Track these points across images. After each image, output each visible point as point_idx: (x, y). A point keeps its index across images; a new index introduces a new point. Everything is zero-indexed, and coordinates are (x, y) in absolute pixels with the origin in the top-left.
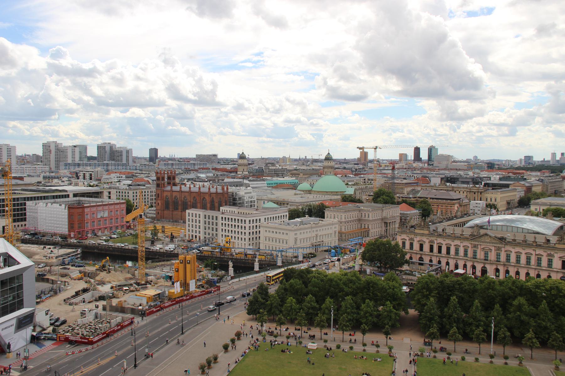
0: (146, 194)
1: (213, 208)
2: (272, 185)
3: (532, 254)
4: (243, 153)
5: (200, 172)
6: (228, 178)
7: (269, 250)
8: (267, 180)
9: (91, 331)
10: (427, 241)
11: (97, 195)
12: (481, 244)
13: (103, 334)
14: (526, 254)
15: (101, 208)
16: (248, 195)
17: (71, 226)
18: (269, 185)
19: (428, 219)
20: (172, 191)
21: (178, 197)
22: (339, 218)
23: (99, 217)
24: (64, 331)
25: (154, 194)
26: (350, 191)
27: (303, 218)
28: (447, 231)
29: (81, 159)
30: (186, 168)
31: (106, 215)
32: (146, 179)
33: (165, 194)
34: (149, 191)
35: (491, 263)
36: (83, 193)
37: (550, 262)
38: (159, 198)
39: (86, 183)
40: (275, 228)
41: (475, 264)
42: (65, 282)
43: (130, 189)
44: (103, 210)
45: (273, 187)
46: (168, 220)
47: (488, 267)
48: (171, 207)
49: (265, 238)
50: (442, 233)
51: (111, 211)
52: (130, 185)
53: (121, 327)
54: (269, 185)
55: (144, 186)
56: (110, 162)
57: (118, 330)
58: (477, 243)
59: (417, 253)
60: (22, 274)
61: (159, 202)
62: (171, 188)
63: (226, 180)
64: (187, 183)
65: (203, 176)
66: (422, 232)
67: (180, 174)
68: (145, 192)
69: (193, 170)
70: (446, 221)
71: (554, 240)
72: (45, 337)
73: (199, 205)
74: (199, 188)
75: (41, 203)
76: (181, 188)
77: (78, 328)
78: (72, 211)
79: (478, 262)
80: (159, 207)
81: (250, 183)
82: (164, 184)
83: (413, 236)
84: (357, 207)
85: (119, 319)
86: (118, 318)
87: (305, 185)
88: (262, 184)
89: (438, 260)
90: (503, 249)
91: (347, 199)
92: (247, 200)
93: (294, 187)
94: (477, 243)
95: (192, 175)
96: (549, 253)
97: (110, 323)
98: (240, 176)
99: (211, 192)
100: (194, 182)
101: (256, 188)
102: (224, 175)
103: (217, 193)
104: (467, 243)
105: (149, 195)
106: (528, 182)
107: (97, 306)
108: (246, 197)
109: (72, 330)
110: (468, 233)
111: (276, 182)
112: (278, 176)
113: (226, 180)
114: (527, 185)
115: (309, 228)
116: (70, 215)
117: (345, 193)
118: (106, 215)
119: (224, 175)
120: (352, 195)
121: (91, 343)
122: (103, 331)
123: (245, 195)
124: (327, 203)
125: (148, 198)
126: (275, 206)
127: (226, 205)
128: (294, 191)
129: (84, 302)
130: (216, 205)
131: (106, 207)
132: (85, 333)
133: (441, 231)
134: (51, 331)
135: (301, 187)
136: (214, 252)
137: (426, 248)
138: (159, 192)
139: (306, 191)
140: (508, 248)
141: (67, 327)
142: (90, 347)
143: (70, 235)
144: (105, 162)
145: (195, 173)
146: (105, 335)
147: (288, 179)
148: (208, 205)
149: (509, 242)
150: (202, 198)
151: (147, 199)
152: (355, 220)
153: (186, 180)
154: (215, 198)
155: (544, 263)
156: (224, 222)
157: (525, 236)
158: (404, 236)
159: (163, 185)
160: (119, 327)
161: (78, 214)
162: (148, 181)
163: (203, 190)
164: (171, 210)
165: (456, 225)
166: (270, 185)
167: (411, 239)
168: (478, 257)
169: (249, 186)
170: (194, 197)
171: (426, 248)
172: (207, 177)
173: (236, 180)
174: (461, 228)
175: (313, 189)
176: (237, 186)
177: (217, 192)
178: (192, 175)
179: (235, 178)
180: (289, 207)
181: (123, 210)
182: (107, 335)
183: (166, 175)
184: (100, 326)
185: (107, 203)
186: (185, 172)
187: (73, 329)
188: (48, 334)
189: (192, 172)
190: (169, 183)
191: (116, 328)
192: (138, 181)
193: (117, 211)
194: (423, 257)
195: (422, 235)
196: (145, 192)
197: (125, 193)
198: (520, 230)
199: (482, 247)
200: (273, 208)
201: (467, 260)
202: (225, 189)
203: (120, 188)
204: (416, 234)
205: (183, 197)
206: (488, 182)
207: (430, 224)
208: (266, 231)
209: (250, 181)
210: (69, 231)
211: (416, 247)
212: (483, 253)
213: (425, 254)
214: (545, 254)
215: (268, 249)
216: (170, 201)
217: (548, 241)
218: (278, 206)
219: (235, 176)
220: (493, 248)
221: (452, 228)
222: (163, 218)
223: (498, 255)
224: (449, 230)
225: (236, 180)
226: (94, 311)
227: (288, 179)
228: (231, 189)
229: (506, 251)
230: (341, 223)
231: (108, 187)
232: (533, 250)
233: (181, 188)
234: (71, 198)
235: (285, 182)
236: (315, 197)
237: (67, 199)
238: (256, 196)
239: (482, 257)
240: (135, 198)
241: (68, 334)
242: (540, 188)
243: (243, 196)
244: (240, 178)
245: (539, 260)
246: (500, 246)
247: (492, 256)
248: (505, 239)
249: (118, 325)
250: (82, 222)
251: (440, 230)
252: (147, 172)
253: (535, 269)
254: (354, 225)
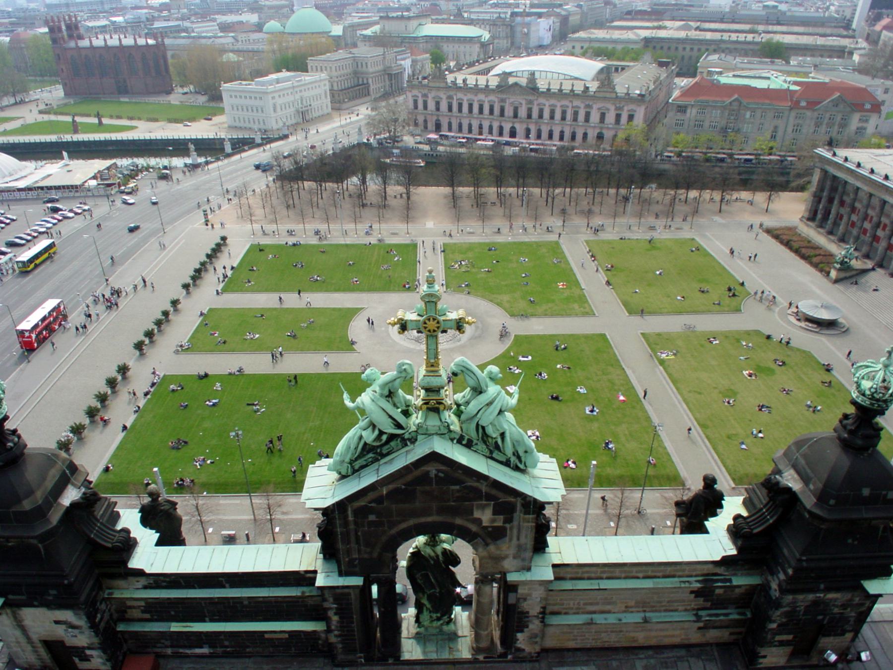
3: (568, 107)
10: (444, 97)
12: (510, 97)
14: (561, 106)
19: (444, 67)
28: (468, 82)
35: (521, 122)
37: (588, 115)
41: (503, 124)
47: (517, 126)
50: (462, 85)
58: (504, 96)
59: (432, 115)
66: (437, 85)
70: (467, 68)
71: (593, 87)
79: (505, 121)
83: (426, 91)
89: (458, 121)
90: (535, 103)
94: (504, 96)
96: (587, 103)
104: (492, 98)
106: (565, 10)
110: (494, 82)
114: (563, 13)
120: (339, 37)
133: (461, 82)
137: (444, 106)
140: (542, 100)
149: (543, 93)
155: (581, 117)
157: (561, 83)
158: (415, 92)
165: (478, 73)
167: (425, 96)
168: (506, 114)
171: (444, 106)
174: (485, 77)
194: (440, 118)
195: (438, 88)
198: (555, 76)
199: (512, 100)
201: (493, 119)
204: (430, 89)
206: (516, 10)
207: (447, 73)
211: (431, 105)
212: (512, 109)
213: (443, 115)
214: (582, 106)
217: (587, 88)
220: (524, 102)
221: (475, 77)
223: (530, 111)
224: (471, 81)
229: (538, 105)
232: (571, 102)
239: (511, 114)
242: (579, 17)
245: (576, 114)
246: (531, 98)
247: (523, 113)
248: (538, 89)
251: (460, 82)
253: (571, 125)
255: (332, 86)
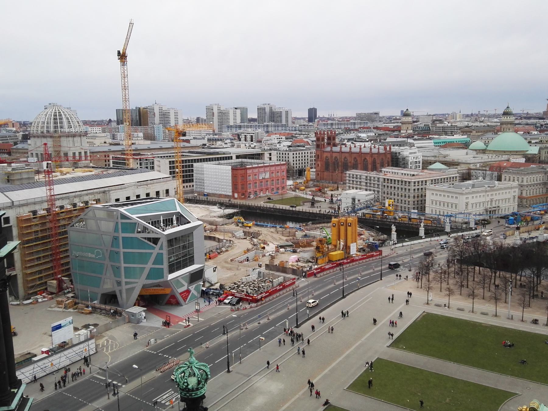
0: (306, 155)
1: (374, 169)
2: (440, 144)
4: (407, 110)
5: (360, 132)
6: (390, 137)
7: (435, 214)
8: (433, 138)
9: (255, 289)
11: (258, 156)
13: (266, 293)
15: (262, 170)
16: (413, 155)
17: (235, 188)
18: (436, 144)
20: (332, 152)
21: (338, 158)
22: (520, 180)
23: (261, 178)
24: (230, 287)
25: (314, 155)
26: (534, 150)
27: (475, 181)
29: (242, 121)
30: (346, 128)
31: (267, 176)
32: (306, 140)
33: (325, 155)
34: (309, 152)
36: (245, 155)
38: (319, 159)
39: (247, 145)
40: (443, 191)
42: (230, 241)
43: (290, 151)
44: (265, 172)
45: (441, 146)
46: (328, 182)
48: (331, 168)
49: (431, 202)
51: (273, 173)
52: (289, 146)
53: (283, 286)
54: (436, 144)
55: (304, 147)
56: (270, 124)
57: (280, 290)
60: (193, 233)
61: (319, 163)
62: (331, 148)
63: (389, 140)
64: (347, 143)
65: (363, 135)
67: (340, 134)
68: (305, 153)
69: (353, 130)
72: (213, 292)
73: (359, 166)
74: (360, 149)
75: (205, 165)
76: (341, 148)
77: (242, 285)
78: (235, 172)
80: (319, 168)
81: (415, 142)
82: (324, 145)
84: (543, 168)
85: (281, 279)
86: (280, 278)
87: (479, 144)
88: (428, 143)
91: (530, 159)
92: (411, 161)
93: (465, 146)
95: (352, 135)
97: (272, 282)
98: (403, 135)
99: (373, 153)
100: (354, 143)
101: (421, 147)
102: (386, 134)
103: (378, 153)
105: (309, 157)
107: (260, 265)
108: (410, 158)
109: (237, 287)
111: (444, 141)
112: (446, 134)
113: (389, 140)
115: (482, 192)
116: (234, 176)
117: (527, 153)
118: (267, 176)
119: (386, 134)
120: (536, 154)
121: (256, 301)
122: (265, 290)
123: (410, 155)
124: (505, 164)
125: (308, 159)
126: (443, 167)
127: (388, 166)
128: (465, 151)
129: (248, 260)
130: (378, 165)
131: (268, 169)
132: (249, 291)
134: (219, 288)
135: (472, 146)
136: (375, 214)
138: (319, 153)
139: (480, 150)
141: (233, 284)
142: (254, 305)
143: (233, 196)
144: (265, 124)
145: (355, 132)
146: (268, 294)
147: (458, 137)
148: (370, 166)
150: (363, 159)
151: (306, 160)
152: (540, 184)
153: (346, 141)
154: (376, 158)
156: (385, 184)
159: (323, 146)
160: (281, 287)
161: (241, 175)
162: (308, 142)
163: (363, 150)
164: (331, 171)
166: (438, 144)
169: (414, 146)
170: (355, 158)
172: (368, 137)
173: (399, 139)
175: (487, 149)
176: (400, 146)
177: (379, 152)
178: (352, 135)
179: (398, 137)
180: (459, 168)
181: (283, 171)
182: (271, 294)
183: (326, 135)
184: (263, 284)
185: (268, 164)
186: (345, 132)
187: (238, 287)
188: (216, 289)
189: (352, 132)
190: (329, 144)
191: (278, 288)
192: (297, 142)
193: (278, 172)
196: (305, 153)
197: (285, 154)
200: (440, 170)
202: (388, 149)
203: (280, 149)
205: (343, 157)
208: (433, 194)
209: (415, 140)
210: (233, 192)
215: (434, 213)
216: (330, 161)
218: (446, 167)
219: (398, 135)
222: (323, 180)
225: (399, 139)
226: (258, 270)
227: (458, 137)
228: (395, 149)
230: (522, 187)
231: (268, 148)
233: (341, 148)
234: (234, 160)
235: (455, 141)
236: (490, 157)
237: (230, 161)
238: (421, 156)
240: (295, 159)
241: (234, 291)
243: (407, 157)
244: (404, 138)
249: (280, 284)
250: (245, 183)
252: (307, 133)
254: (538, 190)
255: (522, 193)
